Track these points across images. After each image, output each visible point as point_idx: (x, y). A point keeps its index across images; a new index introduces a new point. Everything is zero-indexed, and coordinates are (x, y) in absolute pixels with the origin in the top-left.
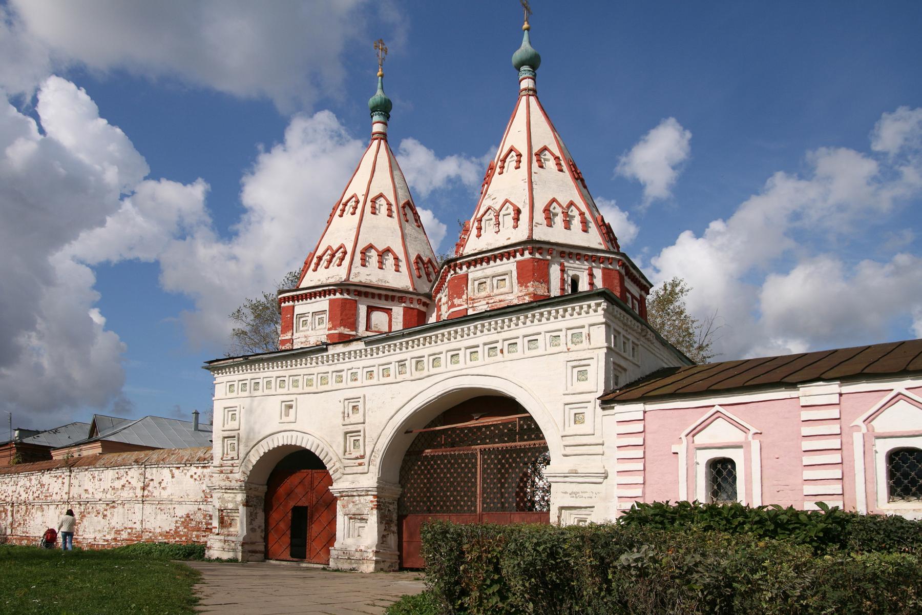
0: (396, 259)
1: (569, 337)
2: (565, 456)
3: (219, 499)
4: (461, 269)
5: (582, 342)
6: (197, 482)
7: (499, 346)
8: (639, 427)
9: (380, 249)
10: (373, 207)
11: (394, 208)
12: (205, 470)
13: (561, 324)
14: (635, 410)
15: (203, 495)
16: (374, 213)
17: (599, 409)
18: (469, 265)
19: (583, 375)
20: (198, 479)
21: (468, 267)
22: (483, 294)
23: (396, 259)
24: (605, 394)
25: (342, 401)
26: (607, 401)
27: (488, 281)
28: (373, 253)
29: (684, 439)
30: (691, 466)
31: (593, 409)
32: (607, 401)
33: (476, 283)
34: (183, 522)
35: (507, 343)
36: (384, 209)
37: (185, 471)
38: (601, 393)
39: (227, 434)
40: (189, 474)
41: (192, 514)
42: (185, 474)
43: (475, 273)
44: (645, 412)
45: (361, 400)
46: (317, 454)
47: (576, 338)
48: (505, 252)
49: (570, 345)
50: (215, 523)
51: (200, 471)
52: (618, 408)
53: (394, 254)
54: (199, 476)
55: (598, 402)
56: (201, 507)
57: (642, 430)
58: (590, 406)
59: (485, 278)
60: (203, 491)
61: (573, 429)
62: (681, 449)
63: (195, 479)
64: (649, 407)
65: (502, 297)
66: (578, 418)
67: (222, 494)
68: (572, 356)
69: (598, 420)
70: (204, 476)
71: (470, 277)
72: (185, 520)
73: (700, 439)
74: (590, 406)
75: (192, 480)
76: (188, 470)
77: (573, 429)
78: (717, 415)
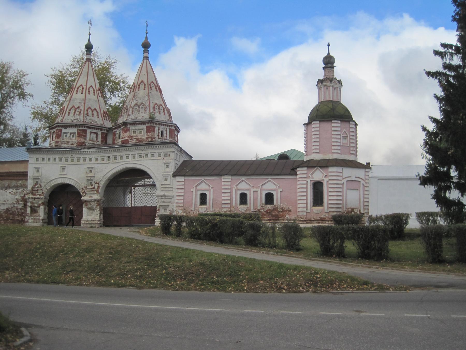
0: (98, 113)
1: (164, 154)
2: (162, 190)
4: (128, 125)
5: (167, 156)
6: (13, 195)
7: (142, 155)
8: (183, 183)
9: (93, 108)
10: (89, 92)
11: (95, 91)
12: (18, 190)
13: (162, 150)
14: (182, 179)
15: (16, 200)
16: (89, 94)
17: (172, 177)
18: (130, 124)
19: (167, 167)
20: (14, 194)
21: (130, 125)
22: (135, 135)
23: (98, 113)
24: (174, 173)
25: (86, 168)
26: (175, 175)
27: (137, 131)
28: (90, 110)
29: (194, 188)
30: (196, 195)
31: (170, 178)
32: (175, 175)
33: (133, 131)
34: (5, 212)
35: (145, 154)
36: (92, 92)
37: (6, 190)
38: (172, 173)
39: (35, 177)
40: (8, 192)
41: (10, 208)
42: (6, 192)
43: (132, 128)
44: (185, 179)
45: (94, 169)
46: (76, 186)
47: (166, 155)
48: (143, 123)
49: (164, 157)
50: (29, 210)
51: (14, 191)
52: (177, 178)
53: (97, 111)
54: (14, 193)
55: (172, 175)
56: (16, 205)
57: (184, 184)
58: (169, 176)
59: (136, 130)
60: (17, 199)
61: (164, 182)
62: (194, 190)
63: (12, 194)
64: (187, 178)
65: (141, 137)
66: (166, 179)
68: (165, 161)
69: (172, 180)
70: (17, 193)
71: (131, 128)
72: (6, 211)
73: (199, 187)
74: (169, 176)
75: (10, 195)
76: (8, 190)
77: (164, 182)
78: (203, 181)
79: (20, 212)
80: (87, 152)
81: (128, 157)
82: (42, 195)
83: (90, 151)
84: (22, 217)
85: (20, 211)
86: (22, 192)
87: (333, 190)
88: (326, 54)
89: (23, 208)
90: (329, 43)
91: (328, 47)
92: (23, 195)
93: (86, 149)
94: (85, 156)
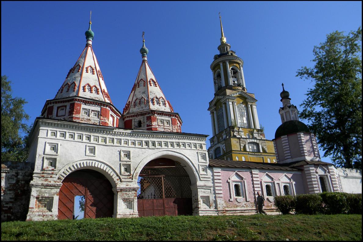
3: (37, 191)
67: (40, 189)
79: (7, 207)
80: (123, 133)
81: (166, 144)
82: (58, 181)
83: (126, 133)
84: (9, 215)
85: (5, 205)
86: (14, 177)
87: (328, 181)
88: (282, 90)
89: (12, 200)
90: (282, 83)
91: (282, 86)
92: (14, 182)
93: (122, 130)
94: (119, 137)
